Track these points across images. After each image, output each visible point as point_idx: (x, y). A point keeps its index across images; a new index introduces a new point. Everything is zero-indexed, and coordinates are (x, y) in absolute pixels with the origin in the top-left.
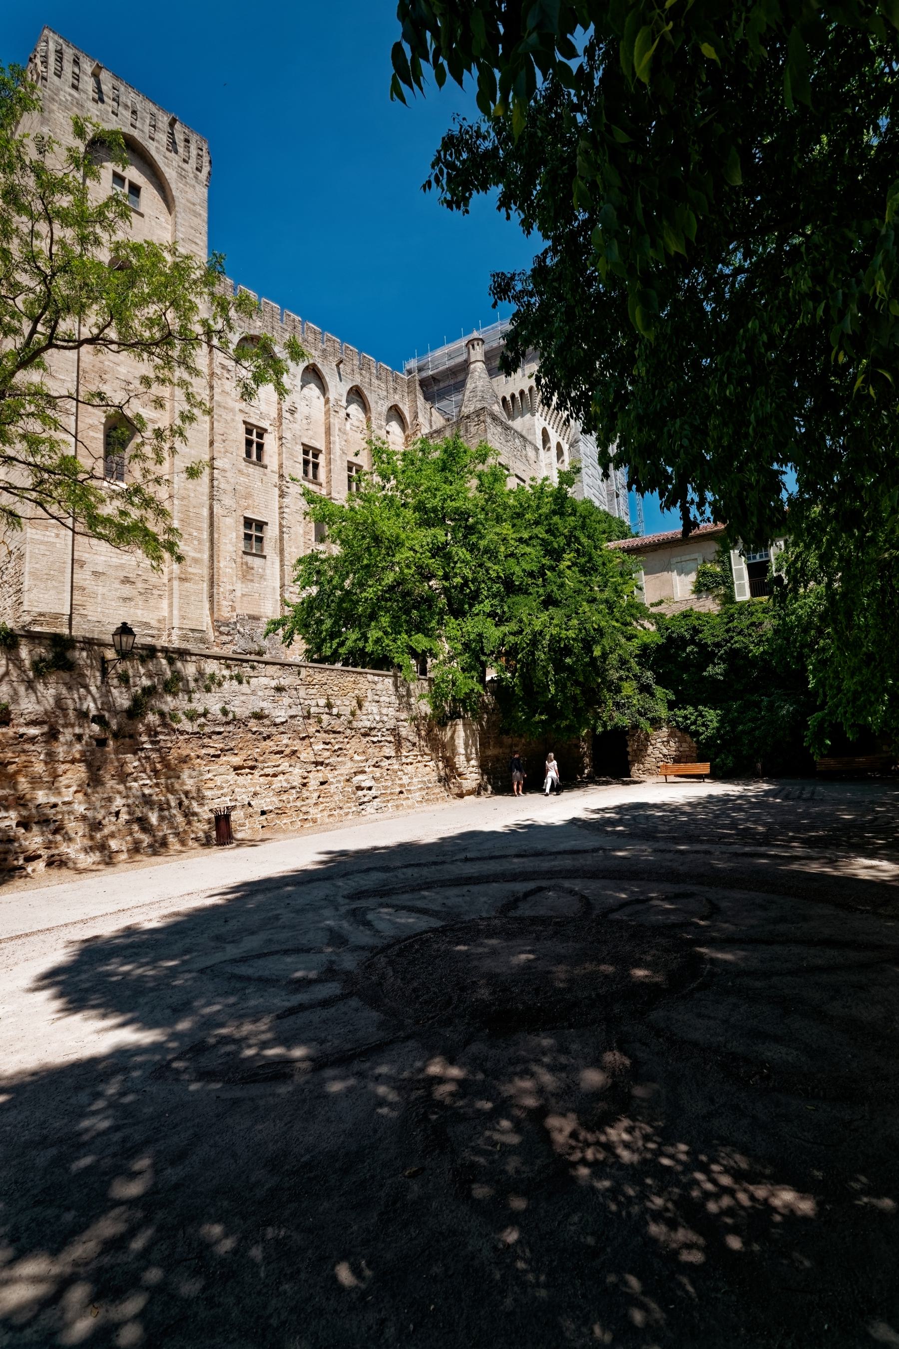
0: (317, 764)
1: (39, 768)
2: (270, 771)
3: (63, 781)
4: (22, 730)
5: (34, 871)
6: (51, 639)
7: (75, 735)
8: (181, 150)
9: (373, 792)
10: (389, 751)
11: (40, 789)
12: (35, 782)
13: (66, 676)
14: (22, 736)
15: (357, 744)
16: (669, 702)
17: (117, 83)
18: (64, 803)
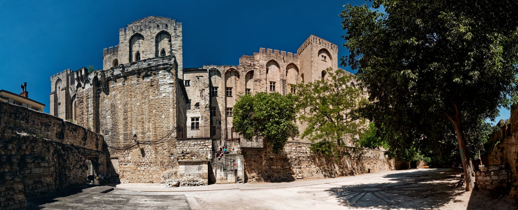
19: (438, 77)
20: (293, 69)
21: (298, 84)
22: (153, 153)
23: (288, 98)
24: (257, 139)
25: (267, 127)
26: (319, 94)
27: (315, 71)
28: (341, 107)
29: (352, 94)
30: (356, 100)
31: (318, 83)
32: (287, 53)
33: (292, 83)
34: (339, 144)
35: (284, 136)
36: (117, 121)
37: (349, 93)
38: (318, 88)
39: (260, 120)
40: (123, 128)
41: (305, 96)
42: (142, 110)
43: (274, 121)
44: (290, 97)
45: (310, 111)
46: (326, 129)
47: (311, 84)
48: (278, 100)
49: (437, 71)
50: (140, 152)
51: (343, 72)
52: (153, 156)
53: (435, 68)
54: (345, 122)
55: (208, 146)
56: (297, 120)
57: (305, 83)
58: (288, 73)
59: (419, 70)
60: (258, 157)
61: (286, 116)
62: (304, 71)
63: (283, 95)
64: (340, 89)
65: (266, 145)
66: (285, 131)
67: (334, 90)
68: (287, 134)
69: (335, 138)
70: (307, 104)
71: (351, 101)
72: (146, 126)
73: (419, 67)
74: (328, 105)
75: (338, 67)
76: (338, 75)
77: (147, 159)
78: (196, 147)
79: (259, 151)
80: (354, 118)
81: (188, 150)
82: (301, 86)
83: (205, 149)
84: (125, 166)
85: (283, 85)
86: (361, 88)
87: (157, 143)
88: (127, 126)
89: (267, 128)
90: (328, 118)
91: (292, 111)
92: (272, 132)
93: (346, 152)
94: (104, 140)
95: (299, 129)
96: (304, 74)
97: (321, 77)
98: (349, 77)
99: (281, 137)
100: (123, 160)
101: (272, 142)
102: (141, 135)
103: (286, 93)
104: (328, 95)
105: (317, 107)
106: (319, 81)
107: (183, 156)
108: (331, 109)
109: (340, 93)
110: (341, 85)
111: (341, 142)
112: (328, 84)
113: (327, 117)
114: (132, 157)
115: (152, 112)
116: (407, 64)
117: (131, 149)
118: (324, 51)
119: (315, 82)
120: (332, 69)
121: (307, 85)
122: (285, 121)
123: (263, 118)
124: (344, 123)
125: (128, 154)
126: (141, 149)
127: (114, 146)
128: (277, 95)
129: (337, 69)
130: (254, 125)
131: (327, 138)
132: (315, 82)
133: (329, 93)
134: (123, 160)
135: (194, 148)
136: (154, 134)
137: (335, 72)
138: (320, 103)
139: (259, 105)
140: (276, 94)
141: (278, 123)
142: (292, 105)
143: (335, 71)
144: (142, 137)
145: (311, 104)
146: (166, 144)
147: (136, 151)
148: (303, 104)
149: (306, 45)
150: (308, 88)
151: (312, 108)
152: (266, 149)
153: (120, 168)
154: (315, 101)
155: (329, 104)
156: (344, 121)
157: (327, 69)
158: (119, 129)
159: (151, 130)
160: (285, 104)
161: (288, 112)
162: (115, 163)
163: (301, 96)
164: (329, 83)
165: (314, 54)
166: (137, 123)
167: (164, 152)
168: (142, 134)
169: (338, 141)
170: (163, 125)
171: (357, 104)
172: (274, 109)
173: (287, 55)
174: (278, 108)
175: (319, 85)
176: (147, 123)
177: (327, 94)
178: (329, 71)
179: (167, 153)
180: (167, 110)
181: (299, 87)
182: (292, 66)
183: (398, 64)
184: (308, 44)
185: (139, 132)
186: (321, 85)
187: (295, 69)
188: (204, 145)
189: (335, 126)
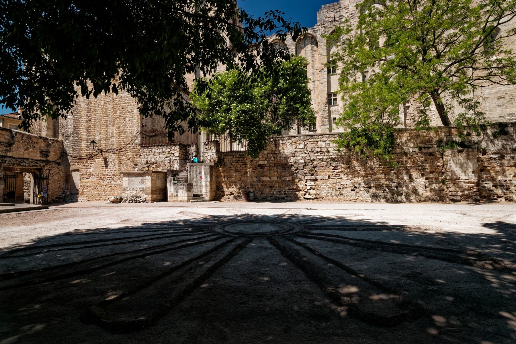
1: (498, 168)
3: (508, 173)
4: (491, 156)
5: (501, 201)
6: (498, 125)
7: (511, 157)
11: (499, 175)
12: (497, 173)
13: (505, 137)
14: (491, 158)
18: (509, 180)
22: (116, 163)
36: (80, 123)
40: (86, 132)
42: (106, 111)
50: (103, 162)
52: (117, 167)
55: (175, 154)
72: (110, 131)
77: (111, 171)
78: (161, 156)
81: (153, 160)
83: (171, 158)
84: (87, 180)
87: (120, 151)
88: (91, 129)
94: (63, 146)
100: (85, 172)
102: (104, 142)
107: (148, 167)
114: (94, 169)
115: (116, 113)
117: (94, 159)
125: (90, 165)
126: (104, 158)
127: (76, 154)
134: (85, 172)
135: (158, 157)
136: (118, 140)
144: (106, 143)
146: (130, 153)
147: (99, 161)
153: (81, 183)
158: (81, 133)
159: (115, 135)
162: (76, 177)
166: (100, 127)
167: (128, 162)
168: (105, 140)
170: (127, 129)
176: (111, 127)
179: (131, 163)
180: (132, 111)
185: (102, 138)
188: (170, 152)
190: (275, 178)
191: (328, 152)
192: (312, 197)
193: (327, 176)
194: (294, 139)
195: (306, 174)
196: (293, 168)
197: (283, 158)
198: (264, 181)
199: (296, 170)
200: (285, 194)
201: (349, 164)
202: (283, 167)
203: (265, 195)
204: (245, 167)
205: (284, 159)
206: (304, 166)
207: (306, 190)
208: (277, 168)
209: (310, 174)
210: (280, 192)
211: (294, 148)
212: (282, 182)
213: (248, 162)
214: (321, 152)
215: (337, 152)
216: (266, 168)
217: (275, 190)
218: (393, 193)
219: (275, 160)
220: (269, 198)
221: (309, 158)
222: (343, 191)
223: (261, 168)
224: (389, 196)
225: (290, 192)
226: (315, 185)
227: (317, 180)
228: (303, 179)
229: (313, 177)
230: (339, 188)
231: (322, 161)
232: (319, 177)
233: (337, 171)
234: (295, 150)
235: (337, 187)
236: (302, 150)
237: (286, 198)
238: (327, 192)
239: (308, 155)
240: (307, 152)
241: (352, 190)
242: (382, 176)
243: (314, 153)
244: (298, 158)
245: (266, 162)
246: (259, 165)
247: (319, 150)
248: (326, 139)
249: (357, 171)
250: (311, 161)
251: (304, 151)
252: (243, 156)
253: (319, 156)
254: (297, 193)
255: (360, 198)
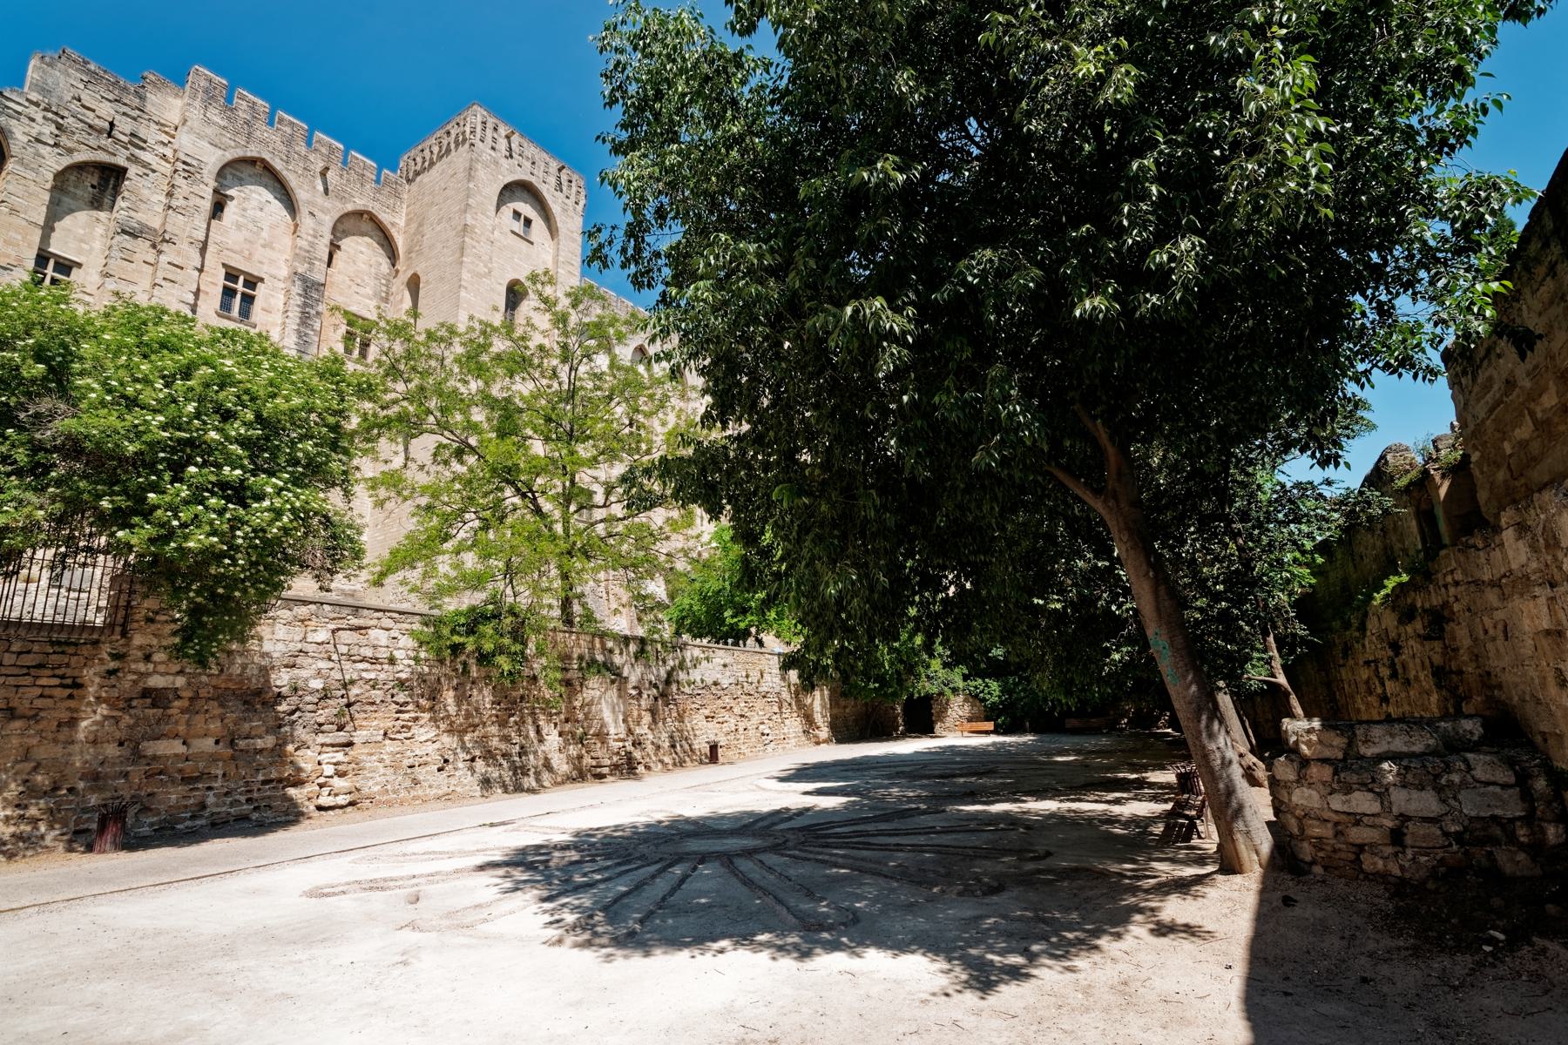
0: (742, 716)
2: (721, 720)
8: (564, 188)
9: (770, 738)
10: (776, 709)
15: (760, 704)
16: (963, 675)
17: (522, 140)
19: (1001, 310)
20: (367, 239)
21: (388, 322)
23: (322, 376)
24: (59, 566)
25: (156, 507)
26: (486, 383)
27: (479, 275)
28: (584, 451)
29: (635, 398)
30: (655, 423)
31: (484, 333)
32: (346, 153)
33: (354, 309)
34: (568, 620)
35: (268, 567)
37: (622, 392)
38: (485, 358)
39: (113, 458)
41: (416, 381)
43: (213, 478)
44: (331, 371)
45: (435, 455)
46: (507, 546)
47: (452, 331)
48: (255, 374)
49: (996, 286)
51: (603, 298)
53: (983, 275)
54: (601, 521)
56: (361, 494)
57: (423, 324)
58: (338, 255)
59: (917, 292)
60: (44, 681)
61: (297, 463)
62: (423, 265)
63: (293, 353)
64: (582, 369)
65: (128, 606)
66: (277, 541)
67: (555, 374)
68: (287, 558)
69: (548, 590)
70: (422, 421)
71: (631, 425)
73: (917, 281)
74: (526, 438)
75: (583, 275)
76: (581, 307)
79: (67, 644)
80: (644, 502)
82: (398, 330)
85: (305, 305)
86: (675, 374)
89: (159, 512)
90: (524, 496)
91: (336, 440)
92: (186, 538)
93: (600, 658)
95: (364, 538)
96: (423, 279)
97: (502, 307)
98: (627, 323)
99: (243, 570)
101: (177, 593)
103: (313, 350)
104: (526, 393)
105: (473, 441)
106: (491, 325)
108: (536, 457)
109: (582, 388)
110: (588, 356)
111: (576, 608)
112: (531, 344)
113: (518, 490)
116: (867, 273)
118: (525, 195)
119: (472, 329)
120: (551, 281)
121: (430, 335)
122: (281, 489)
123: (140, 453)
124: (596, 522)
128: (255, 350)
129: (575, 281)
130: (58, 483)
131: (509, 591)
132: (472, 329)
133: (531, 385)
137: (568, 295)
138: (485, 426)
139: (122, 373)
140: (250, 341)
141: (239, 494)
142: (339, 413)
143: (569, 290)
145: (443, 427)
148: (402, 418)
149: (445, 142)
150: (436, 350)
151: (445, 441)
152: (124, 634)
154: (465, 412)
155: (529, 432)
156: (599, 514)
157: (534, 278)
160: (297, 401)
161: (308, 445)
163: (394, 381)
164: (536, 340)
165: (479, 198)
169: (566, 604)
171: (659, 440)
172: (228, 416)
173: (345, 162)
174: (250, 416)
175: (491, 345)
177: (523, 388)
178: (539, 286)
181: (388, 332)
182: (363, 222)
183: (833, 275)
184: (457, 144)
186: (499, 345)
187: (382, 246)
189: (554, 538)
190: (208, 744)
191: (392, 661)
192: (341, 800)
193: (382, 732)
194: (303, 611)
195: (320, 725)
196: (283, 707)
197: (252, 671)
198: (155, 758)
199: (292, 713)
200: (249, 800)
201: (434, 699)
202: (245, 703)
203: (159, 814)
204: (71, 697)
205: (256, 672)
206: (320, 699)
207: (322, 780)
208: (222, 705)
209: (335, 727)
210: (227, 794)
211: (298, 638)
212: (233, 758)
213: (91, 676)
214: (374, 661)
215: (412, 662)
216: (176, 703)
217: (210, 788)
218: (514, 769)
219: (223, 677)
220: (188, 823)
221: (338, 676)
222: (420, 773)
223: (154, 705)
224: (507, 776)
225: (267, 791)
226: (346, 759)
227: (350, 744)
228: (310, 743)
229: (342, 737)
230: (410, 767)
231: (373, 687)
232: (359, 737)
233: (406, 716)
234: (299, 646)
235: (406, 762)
236: (321, 647)
237: (255, 816)
238: (383, 779)
239: (338, 666)
240: (335, 657)
241: (440, 770)
242: (494, 729)
243: (354, 662)
244: (304, 673)
245: (180, 681)
246: (146, 693)
247: (368, 652)
248: (387, 623)
249: (448, 716)
250: (345, 686)
251: (327, 652)
252: (71, 650)
253: (366, 670)
254: (292, 791)
255: (459, 789)
